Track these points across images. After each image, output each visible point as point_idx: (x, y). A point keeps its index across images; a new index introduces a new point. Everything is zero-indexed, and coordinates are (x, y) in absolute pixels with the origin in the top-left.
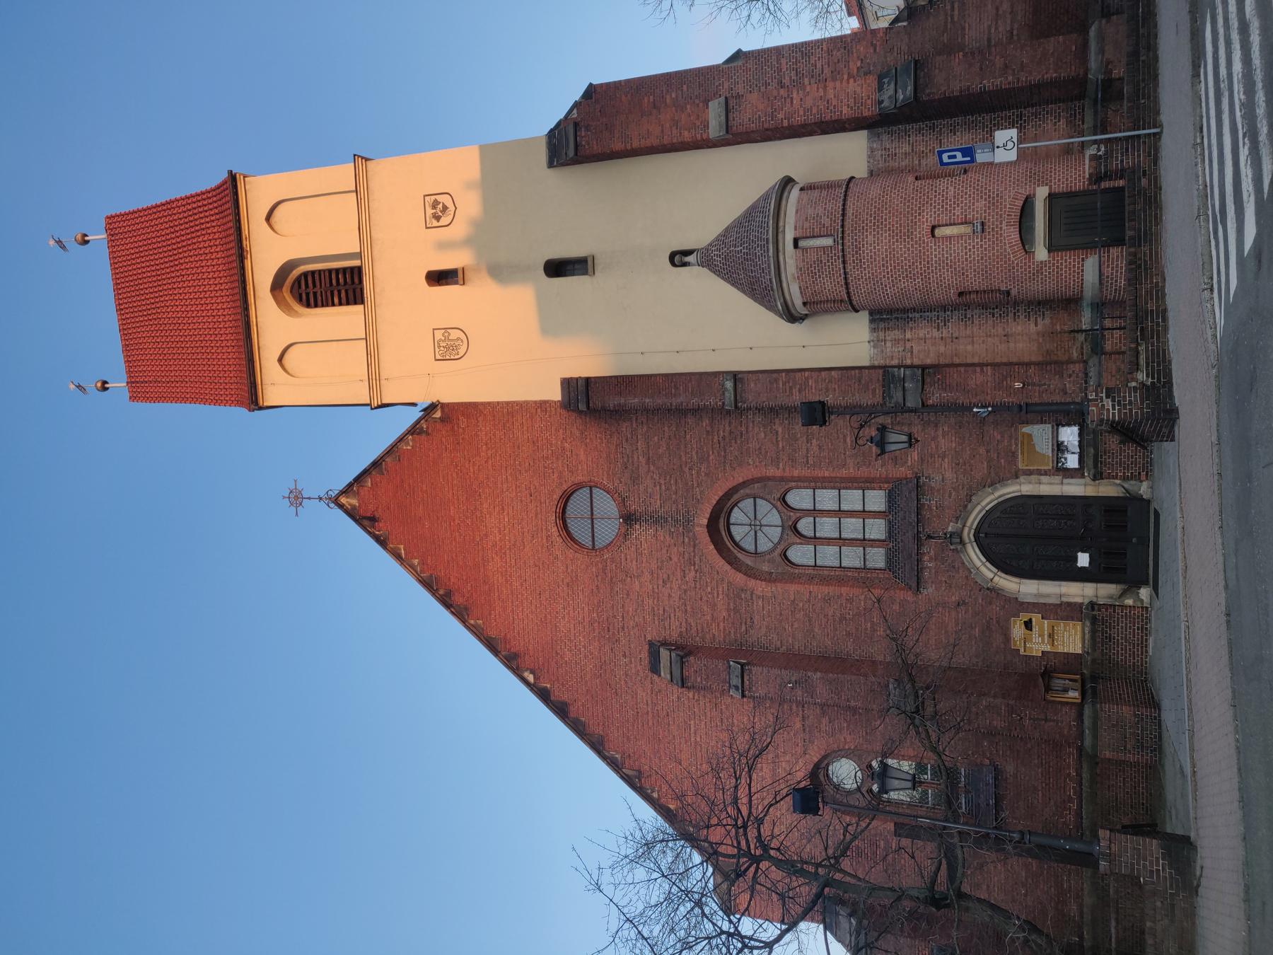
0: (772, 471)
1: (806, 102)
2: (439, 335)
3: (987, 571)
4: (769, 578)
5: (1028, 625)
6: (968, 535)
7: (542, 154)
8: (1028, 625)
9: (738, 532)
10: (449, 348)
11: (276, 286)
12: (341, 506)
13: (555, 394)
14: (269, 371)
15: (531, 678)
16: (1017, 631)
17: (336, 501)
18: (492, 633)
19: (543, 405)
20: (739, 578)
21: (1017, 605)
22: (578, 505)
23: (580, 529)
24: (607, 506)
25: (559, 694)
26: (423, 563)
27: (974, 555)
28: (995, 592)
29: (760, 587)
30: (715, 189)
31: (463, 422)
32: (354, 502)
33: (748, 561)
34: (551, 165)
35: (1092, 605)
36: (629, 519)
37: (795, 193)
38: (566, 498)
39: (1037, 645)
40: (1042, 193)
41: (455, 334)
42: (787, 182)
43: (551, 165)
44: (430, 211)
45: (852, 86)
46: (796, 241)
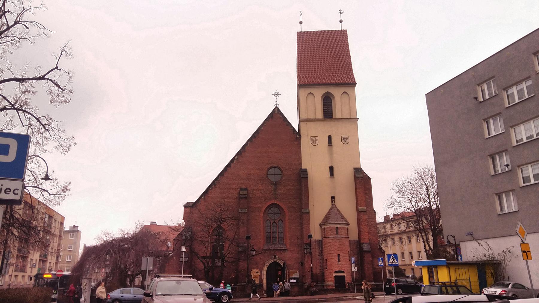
0: (287, 218)
1: (364, 227)
2: (317, 138)
3: (268, 264)
4: (263, 216)
5: (257, 273)
6: (275, 260)
7: (357, 167)
8: (257, 273)
9: (272, 209)
10: (314, 141)
11: (328, 93)
12: (275, 108)
13: (303, 167)
14: (309, 90)
15: (236, 158)
16: (256, 270)
17: (276, 107)
18: (246, 148)
19: (301, 164)
20: (263, 210)
21: (261, 271)
22: (277, 171)
23: (272, 171)
24: (278, 178)
25: (233, 165)
26: (262, 130)
27: (271, 261)
28: (264, 266)
29: (262, 215)
30: (348, 208)
31: (296, 143)
32: (276, 112)
33: (266, 212)
34: (354, 169)
35: (263, 285)
36: (275, 184)
37: (346, 227)
38: (279, 168)
39: (253, 274)
40: (345, 274)
41: (317, 142)
42: (348, 224)
43: (354, 169)
44: (345, 137)
45: (367, 238)
46: (337, 228)
